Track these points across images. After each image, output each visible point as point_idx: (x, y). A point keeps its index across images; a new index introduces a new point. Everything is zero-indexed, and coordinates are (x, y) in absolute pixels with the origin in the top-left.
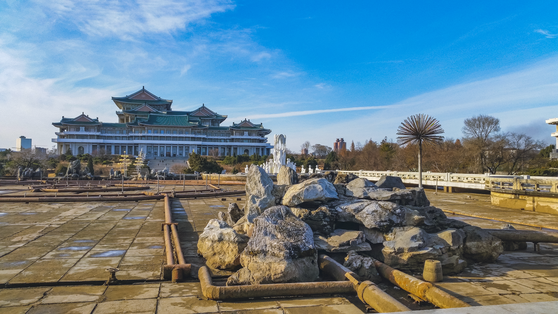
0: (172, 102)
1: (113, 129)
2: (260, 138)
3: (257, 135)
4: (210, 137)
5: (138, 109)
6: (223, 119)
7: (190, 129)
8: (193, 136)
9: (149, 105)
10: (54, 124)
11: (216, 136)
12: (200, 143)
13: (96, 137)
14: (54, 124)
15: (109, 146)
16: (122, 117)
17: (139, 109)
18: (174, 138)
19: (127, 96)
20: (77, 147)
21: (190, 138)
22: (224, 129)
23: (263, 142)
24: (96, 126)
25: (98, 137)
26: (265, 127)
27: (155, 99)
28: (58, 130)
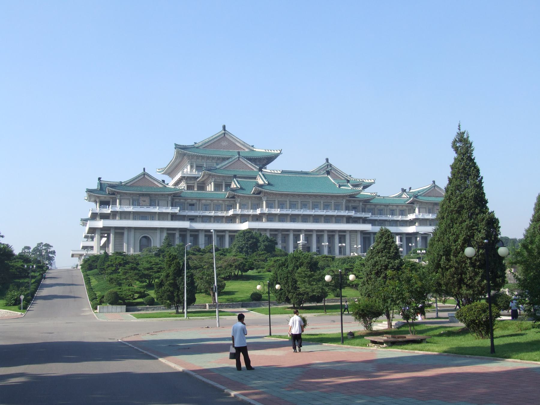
1: (198, 203)
5: (226, 166)
9: (244, 158)
13: (170, 217)
15: (195, 233)
16: (191, 182)
17: (228, 165)
18: (316, 219)
19: (195, 143)
20: (139, 236)
24: (171, 194)
25: (174, 217)
27: (244, 148)
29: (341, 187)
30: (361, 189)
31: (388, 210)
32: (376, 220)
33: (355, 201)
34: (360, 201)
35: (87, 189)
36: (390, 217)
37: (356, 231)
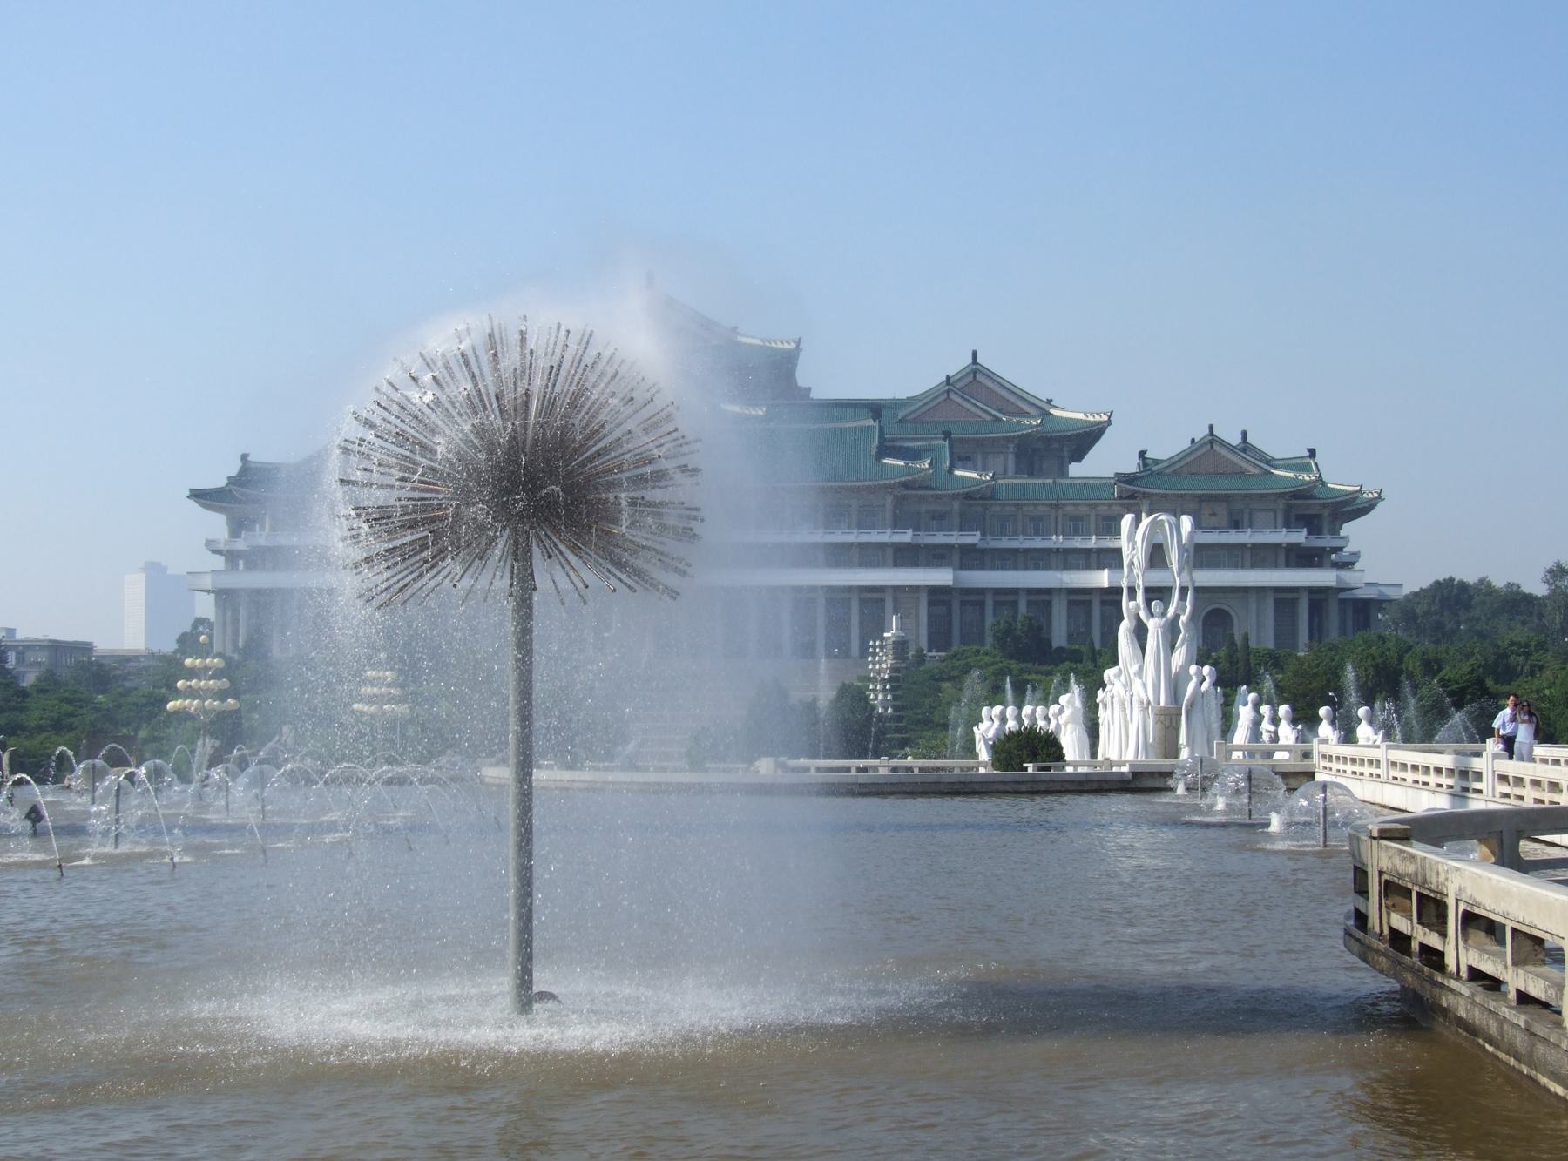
0: (798, 349)
2: (1299, 536)
3: (1280, 521)
4: (1006, 543)
6: (1084, 439)
7: (889, 500)
8: (906, 537)
10: (198, 495)
11: (1037, 533)
12: (942, 577)
14: (198, 495)
21: (890, 552)
22: (1091, 487)
23: (1320, 565)
26: (1339, 478)
28: (216, 524)
29: (886, 461)
30: (927, 466)
31: (1060, 519)
32: (1016, 551)
33: (938, 497)
34: (954, 497)
35: (191, 490)
36: (1057, 541)
37: (915, 589)
